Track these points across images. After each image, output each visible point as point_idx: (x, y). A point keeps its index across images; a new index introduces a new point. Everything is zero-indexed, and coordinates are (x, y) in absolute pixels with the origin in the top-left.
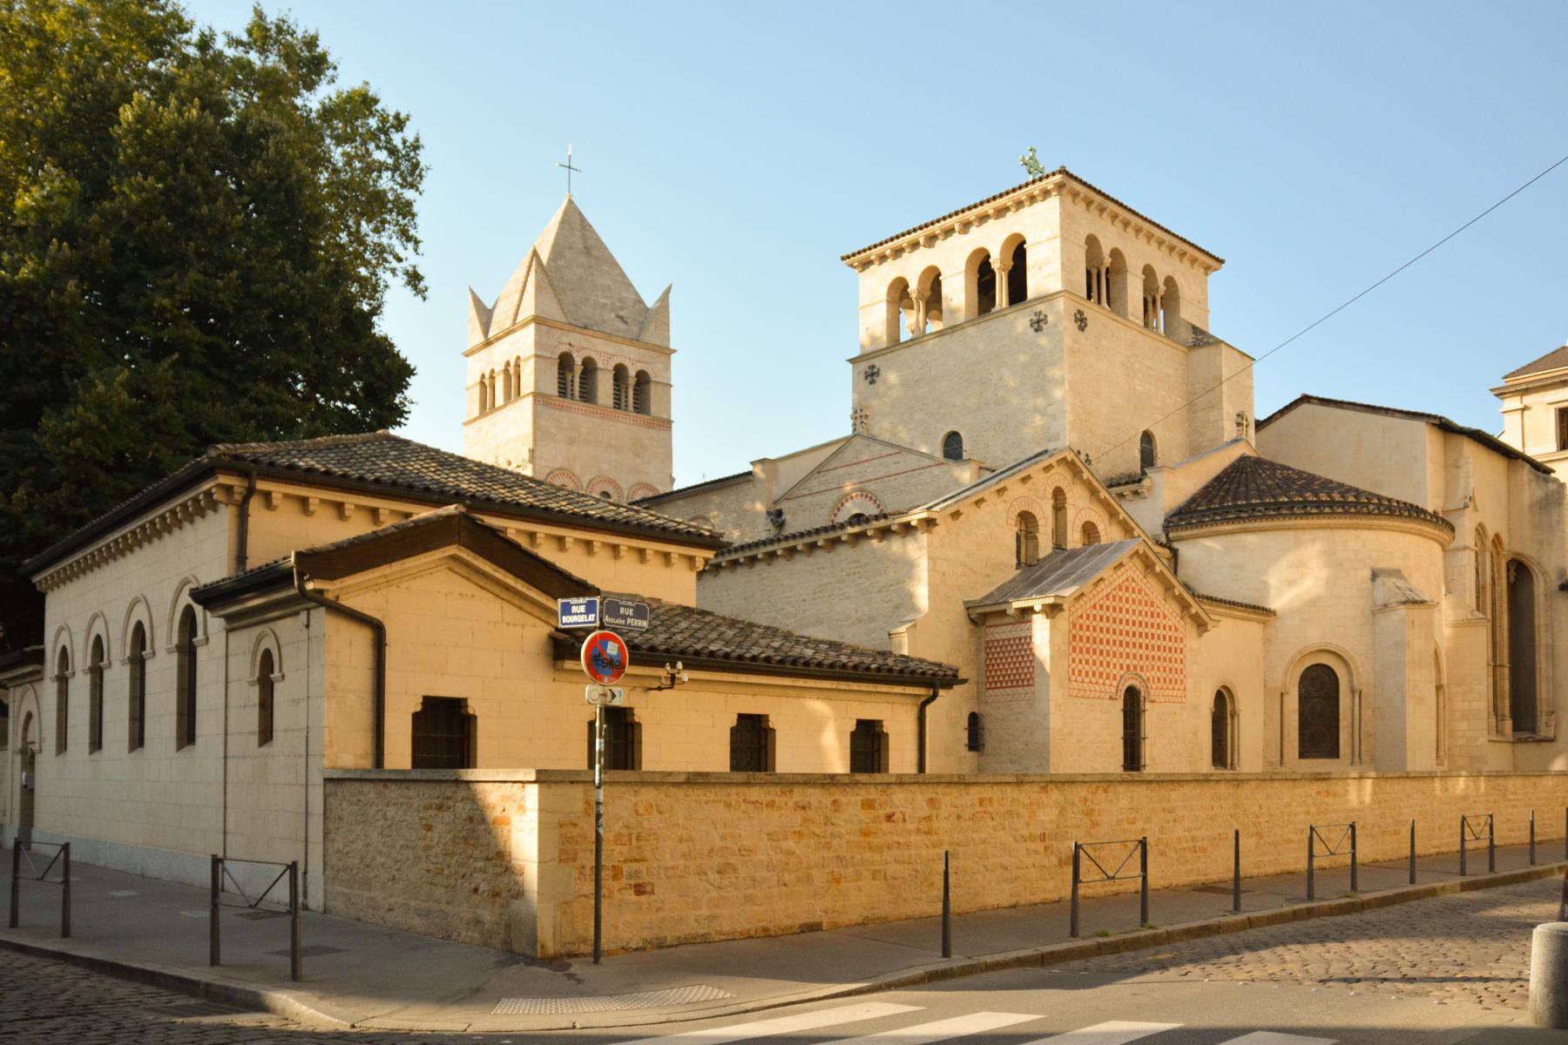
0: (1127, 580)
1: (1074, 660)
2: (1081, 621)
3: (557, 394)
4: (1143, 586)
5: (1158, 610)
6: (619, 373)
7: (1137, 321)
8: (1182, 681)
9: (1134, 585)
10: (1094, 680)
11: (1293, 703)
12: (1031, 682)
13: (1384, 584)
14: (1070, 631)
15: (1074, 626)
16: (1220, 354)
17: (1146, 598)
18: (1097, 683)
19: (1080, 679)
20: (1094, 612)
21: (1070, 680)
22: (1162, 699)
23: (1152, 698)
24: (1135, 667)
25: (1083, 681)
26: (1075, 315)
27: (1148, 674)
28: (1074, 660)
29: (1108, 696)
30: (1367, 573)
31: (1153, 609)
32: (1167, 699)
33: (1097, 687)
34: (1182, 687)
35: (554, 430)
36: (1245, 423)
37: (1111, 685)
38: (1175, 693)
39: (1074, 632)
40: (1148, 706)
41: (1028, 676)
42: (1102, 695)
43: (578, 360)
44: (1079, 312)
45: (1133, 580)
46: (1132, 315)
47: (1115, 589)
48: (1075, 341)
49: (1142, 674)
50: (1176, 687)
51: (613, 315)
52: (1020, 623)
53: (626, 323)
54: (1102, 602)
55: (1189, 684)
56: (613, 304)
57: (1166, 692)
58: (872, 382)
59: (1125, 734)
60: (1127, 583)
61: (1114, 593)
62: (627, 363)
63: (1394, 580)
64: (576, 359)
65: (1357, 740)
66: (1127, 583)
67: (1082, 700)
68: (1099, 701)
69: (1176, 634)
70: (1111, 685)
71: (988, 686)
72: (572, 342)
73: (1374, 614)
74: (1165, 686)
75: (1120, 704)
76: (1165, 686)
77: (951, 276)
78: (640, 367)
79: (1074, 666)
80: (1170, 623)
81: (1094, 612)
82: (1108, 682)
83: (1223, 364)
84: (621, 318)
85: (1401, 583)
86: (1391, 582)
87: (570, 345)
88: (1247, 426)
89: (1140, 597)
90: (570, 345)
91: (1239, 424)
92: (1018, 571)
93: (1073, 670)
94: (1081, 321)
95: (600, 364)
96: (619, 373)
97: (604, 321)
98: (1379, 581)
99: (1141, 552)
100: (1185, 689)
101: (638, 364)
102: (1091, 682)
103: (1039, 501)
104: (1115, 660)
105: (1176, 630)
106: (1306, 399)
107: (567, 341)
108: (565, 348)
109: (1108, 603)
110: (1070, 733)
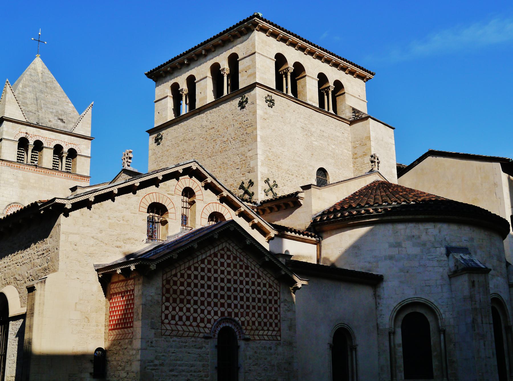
0: (223, 249)
1: (167, 308)
2: (175, 279)
3: (16, 160)
4: (238, 255)
5: (253, 272)
6: (58, 149)
7: (314, 105)
8: (276, 325)
9: (229, 253)
10: (188, 323)
11: (398, 339)
12: (132, 325)
13: (453, 255)
14: (163, 286)
15: (168, 282)
16: (369, 124)
17: (241, 263)
18: (191, 325)
19: (173, 322)
20: (189, 272)
21: (163, 323)
22: (257, 338)
23: (248, 336)
24: (230, 314)
25: (176, 324)
26: (266, 98)
27: (243, 319)
28: (167, 308)
29: (201, 335)
30: (443, 250)
31: (247, 271)
32: (262, 338)
33: (191, 329)
34: (277, 329)
35: (13, 181)
36: (376, 161)
37: (205, 327)
38: (270, 333)
39: (168, 286)
40: (242, 344)
41: (130, 320)
42: (197, 335)
43: (31, 142)
44: (268, 96)
45: (229, 250)
46: (310, 101)
47: (210, 256)
48: (266, 113)
49: (237, 319)
50: (265, 328)
51: (56, 118)
52: (127, 280)
53: (64, 122)
54: (197, 265)
55: (284, 326)
56: (57, 112)
57: (261, 333)
58: (159, 144)
59: (218, 363)
60: (222, 252)
61: (210, 258)
62: (62, 144)
63: (461, 255)
64: (30, 141)
65: (444, 365)
66: (222, 252)
67: (175, 338)
68: (193, 339)
69: (270, 290)
70: (205, 327)
71: (110, 328)
72: (28, 132)
73: (450, 277)
74: (254, 327)
75: (214, 342)
76: (260, 328)
77: (201, 80)
78: (71, 146)
79: (167, 312)
80: (264, 282)
81: (189, 272)
82: (202, 325)
83: (371, 129)
84: (62, 120)
85: (466, 257)
86: (458, 256)
87: (26, 133)
88: (378, 163)
89: (235, 262)
90: (26, 133)
91: (372, 162)
92: (148, 245)
93: (166, 317)
94: (271, 102)
95: (45, 145)
96: (58, 149)
97: (50, 121)
98: (451, 255)
99: (232, 229)
100: (280, 330)
101: (70, 145)
102: (184, 324)
103: (169, 196)
104: (209, 308)
105: (270, 286)
106: (432, 153)
107: (25, 132)
108: (23, 135)
109: (203, 266)
110: (162, 365)
